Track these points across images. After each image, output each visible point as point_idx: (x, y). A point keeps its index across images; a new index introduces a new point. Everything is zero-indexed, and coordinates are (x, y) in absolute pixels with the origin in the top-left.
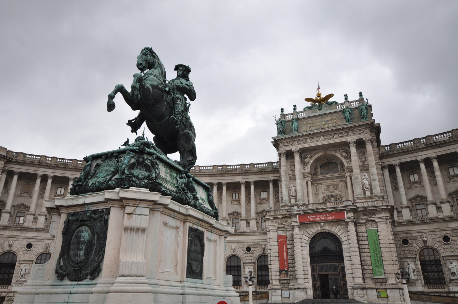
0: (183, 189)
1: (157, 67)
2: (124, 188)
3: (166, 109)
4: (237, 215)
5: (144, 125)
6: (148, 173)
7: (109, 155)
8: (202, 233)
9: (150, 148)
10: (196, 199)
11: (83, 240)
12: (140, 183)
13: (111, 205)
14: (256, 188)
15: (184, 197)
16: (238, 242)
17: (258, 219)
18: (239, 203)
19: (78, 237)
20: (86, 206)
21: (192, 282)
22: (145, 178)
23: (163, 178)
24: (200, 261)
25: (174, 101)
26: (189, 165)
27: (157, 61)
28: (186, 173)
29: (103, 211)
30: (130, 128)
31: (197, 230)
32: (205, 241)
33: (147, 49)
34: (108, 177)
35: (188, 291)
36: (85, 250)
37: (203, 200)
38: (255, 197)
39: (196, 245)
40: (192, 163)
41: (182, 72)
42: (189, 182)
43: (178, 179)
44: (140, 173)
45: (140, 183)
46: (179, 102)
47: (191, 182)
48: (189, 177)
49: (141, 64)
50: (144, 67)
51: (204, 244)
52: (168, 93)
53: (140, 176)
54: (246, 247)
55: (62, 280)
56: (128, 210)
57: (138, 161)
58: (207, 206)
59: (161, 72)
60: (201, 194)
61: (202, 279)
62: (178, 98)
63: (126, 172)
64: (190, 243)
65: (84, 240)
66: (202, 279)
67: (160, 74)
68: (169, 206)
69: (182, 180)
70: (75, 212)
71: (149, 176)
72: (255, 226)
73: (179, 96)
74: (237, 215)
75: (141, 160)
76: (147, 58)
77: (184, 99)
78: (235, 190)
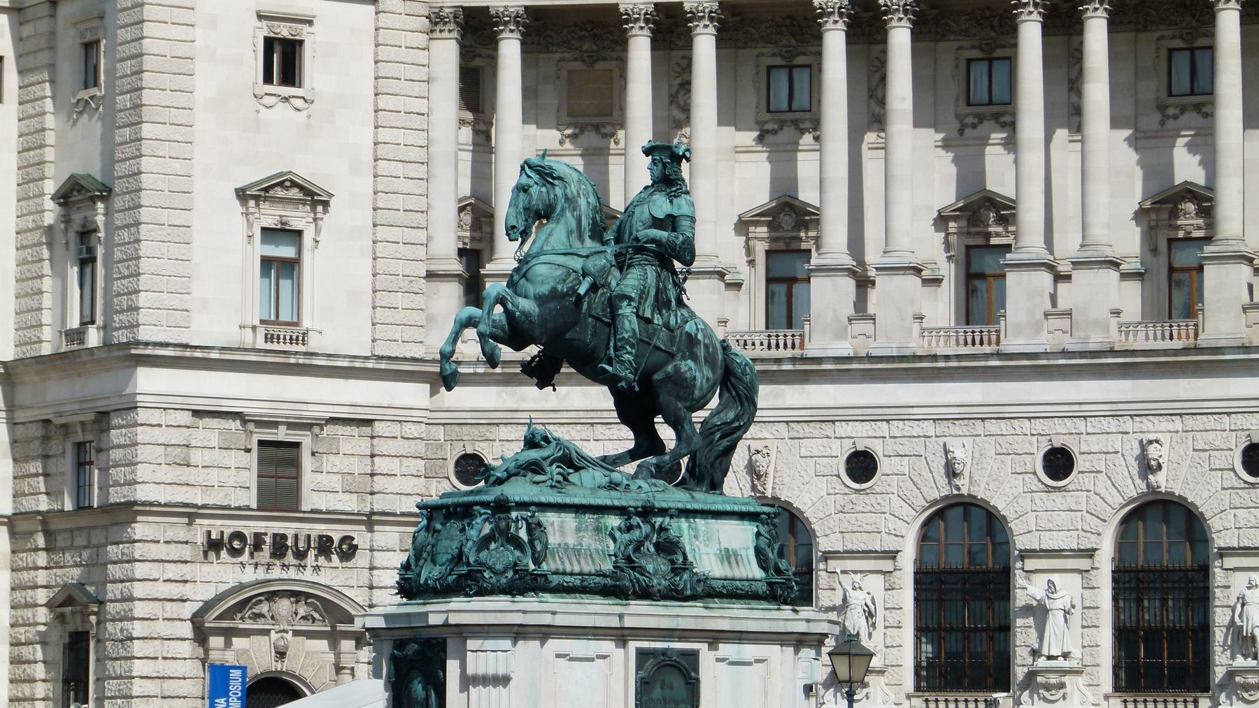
1: (563, 210)
3: (594, 334)
10: (681, 567)
26: (721, 438)
27: (559, 191)
33: (530, 167)
37: (728, 556)
41: (660, 165)
44: (500, 556)
49: (513, 227)
53: (499, 567)
57: (497, 526)
59: (574, 225)
63: (472, 560)
67: (569, 233)
69: (627, 537)
71: (516, 564)
75: (503, 524)
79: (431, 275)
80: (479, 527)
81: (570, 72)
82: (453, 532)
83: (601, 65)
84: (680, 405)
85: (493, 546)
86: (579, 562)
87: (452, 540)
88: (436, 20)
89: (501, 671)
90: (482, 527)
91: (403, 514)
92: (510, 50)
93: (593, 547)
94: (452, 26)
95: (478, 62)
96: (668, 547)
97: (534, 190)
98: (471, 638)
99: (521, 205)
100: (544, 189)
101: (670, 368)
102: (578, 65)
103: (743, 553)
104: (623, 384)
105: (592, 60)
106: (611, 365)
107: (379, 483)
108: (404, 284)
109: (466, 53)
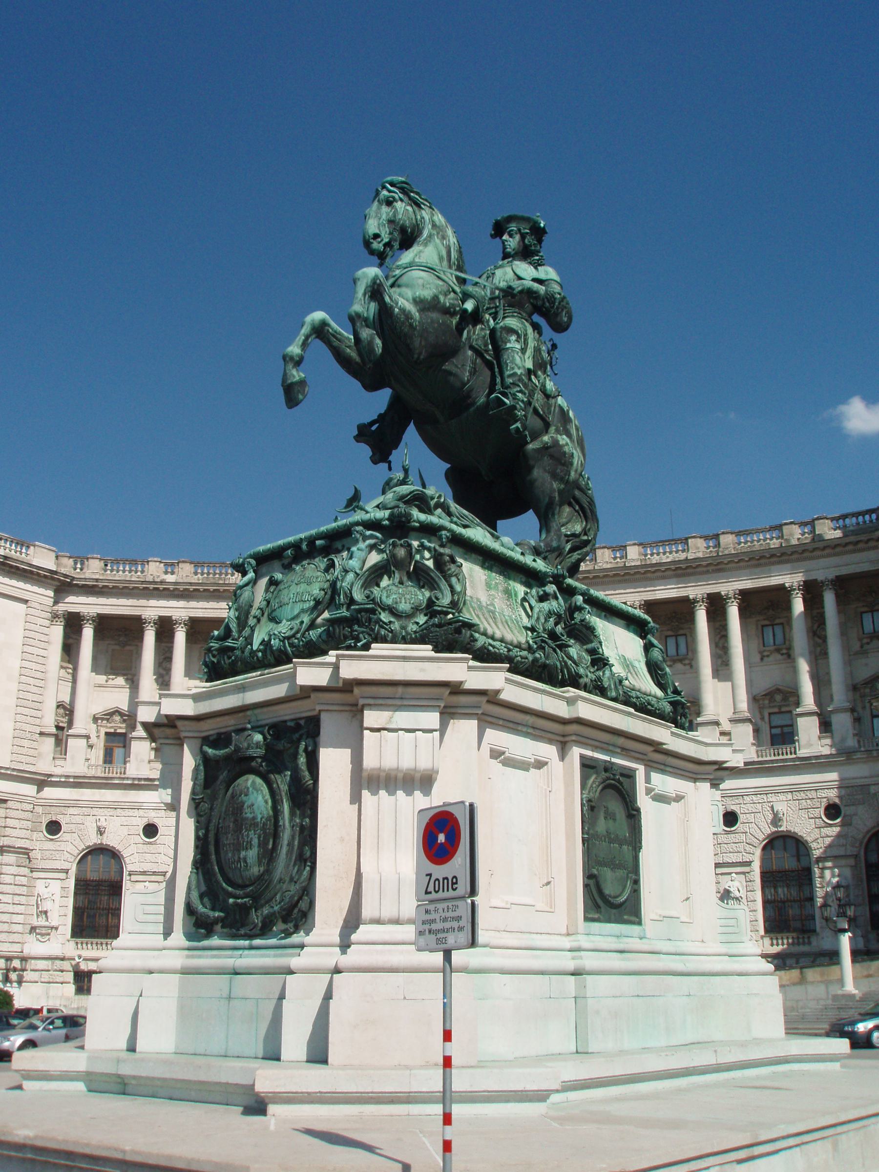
0: (553, 635)
1: (430, 236)
2: (355, 648)
3: (474, 371)
4: (785, 699)
5: (411, 434)
6: (427, 594)
7: (304, 546)
8: (630, 775)
9: (428, 510)
10: (600, 662)
11: (250, 816)
12: (403, 628)
13: (318, 708)
14: (841, 601)
15: (555, 659)
16: (793, 790)
17: (859, 709)
18: (789, 656)
19: (237, 809)
20: (249, 713)
21: (607, 933)
22: (416, 610)
23: (480, 607)
24: (630, 864)
25: (496, 339)
26: (572, 550)
27: (427, 217)
28: (558, 580)
29: (298, 727)
30: (365, 451)
31: (608, 767)
32: (643, 801)
33: (392, 185)
34: (306, 619)
35: (589, 961)
36: (259, 846)
37: (627, 664)
38: (844, 632)
39: (610, 816)
40: (583, 545)
41: (517, 237)
42: (573, 610)
43: (533, 602)
45: (403, 628)
46: (513, 343)
47: (580, 609)
48: (569, 592)
49: (376, 236)
50: (388, 245)
51: (638, 810)
52: (475, 318)
54: (824, 805)
55: (209, 934)
56: (371, 718)
58: (646, 684)
59: (444, 253)
60: (621, 646)
61: (640, 923)
62: (511, 331)
63: (358, 596)
64: (590, 809)
65: (254, 818)
66: (640, 923)
67: (441, 258)
68: (503, 696)
69: (545, 606)
70: (219, 734)
71: (431, 603)
72: (851, 732)
73: (512, 322)
74: (785, 699)
76: (396, 212)
77: (530, 330)
78: (771, 612)
79: (42, 734)
80: (362, 554)
81: (113, 650)
82: (308, 573)
83: (128, 648)
84: (555, 486)
85: (385, 582)
86: (498, 627)
87: (309, 583)
88: (55, 616)
89: (424, 764)
90: (364, 556)
91: (19, 848)
92: (88, 633)
93: (506, 613)
94: (62, 620)
95: (70, 641)
96: (585, 634)
97: (399, 205)
98: (371, 706)
99: (384, 217)
100: (409, 208)
101: (546, 438)
102: (117, 647)
103: (636, 664)
104: (518, 425)
105: (125, 644)
106: (508, 399)
107: (8, 831)
108: (29, 735)
109: (66, 636)
